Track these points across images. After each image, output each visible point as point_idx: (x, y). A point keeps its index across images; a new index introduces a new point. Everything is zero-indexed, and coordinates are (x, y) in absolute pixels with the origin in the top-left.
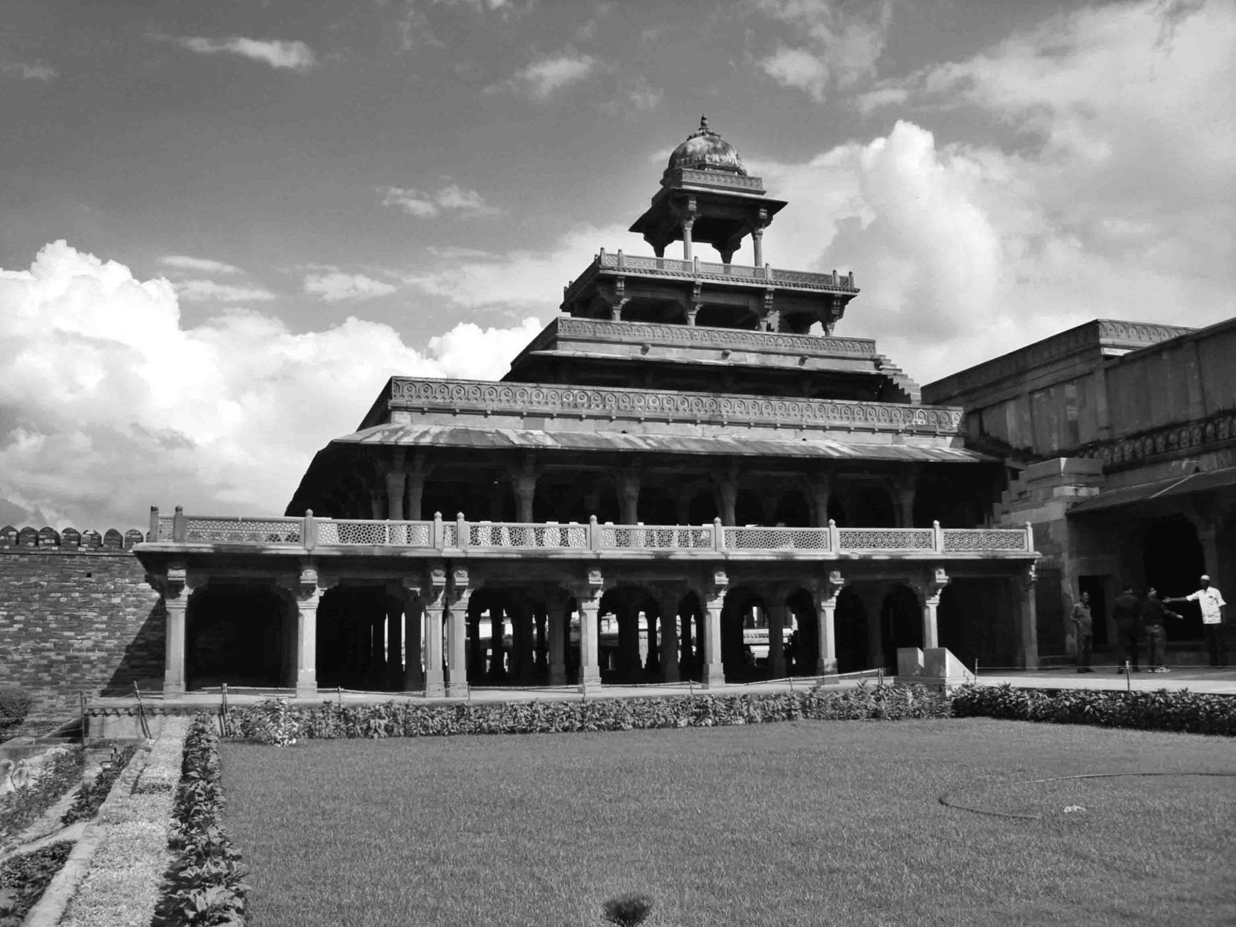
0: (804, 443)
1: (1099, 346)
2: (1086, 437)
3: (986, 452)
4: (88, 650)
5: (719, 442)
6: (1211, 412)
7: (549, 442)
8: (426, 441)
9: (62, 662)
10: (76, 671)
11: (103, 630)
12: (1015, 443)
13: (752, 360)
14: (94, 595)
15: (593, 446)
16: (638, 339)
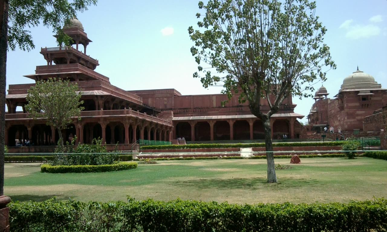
2: (168, 107)
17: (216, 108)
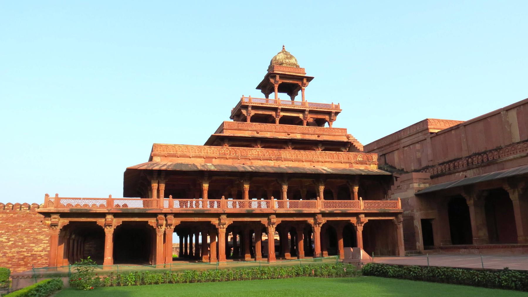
0: (314, 168)
1: (428, 129)
2: (424, 164)
3: (387, 171)
4: (40, 251)
5: (279, 167)
6: (471, 153)
7: (213, 168)
8: (164, 168)
9: (30, 256)
10: (35, 260)
11: (47, 243)
12: (398, 167)
13: (299, 136)
14: (43, 230)
15: (229, 170)
16: (255, 129)
17: (518, 143)
